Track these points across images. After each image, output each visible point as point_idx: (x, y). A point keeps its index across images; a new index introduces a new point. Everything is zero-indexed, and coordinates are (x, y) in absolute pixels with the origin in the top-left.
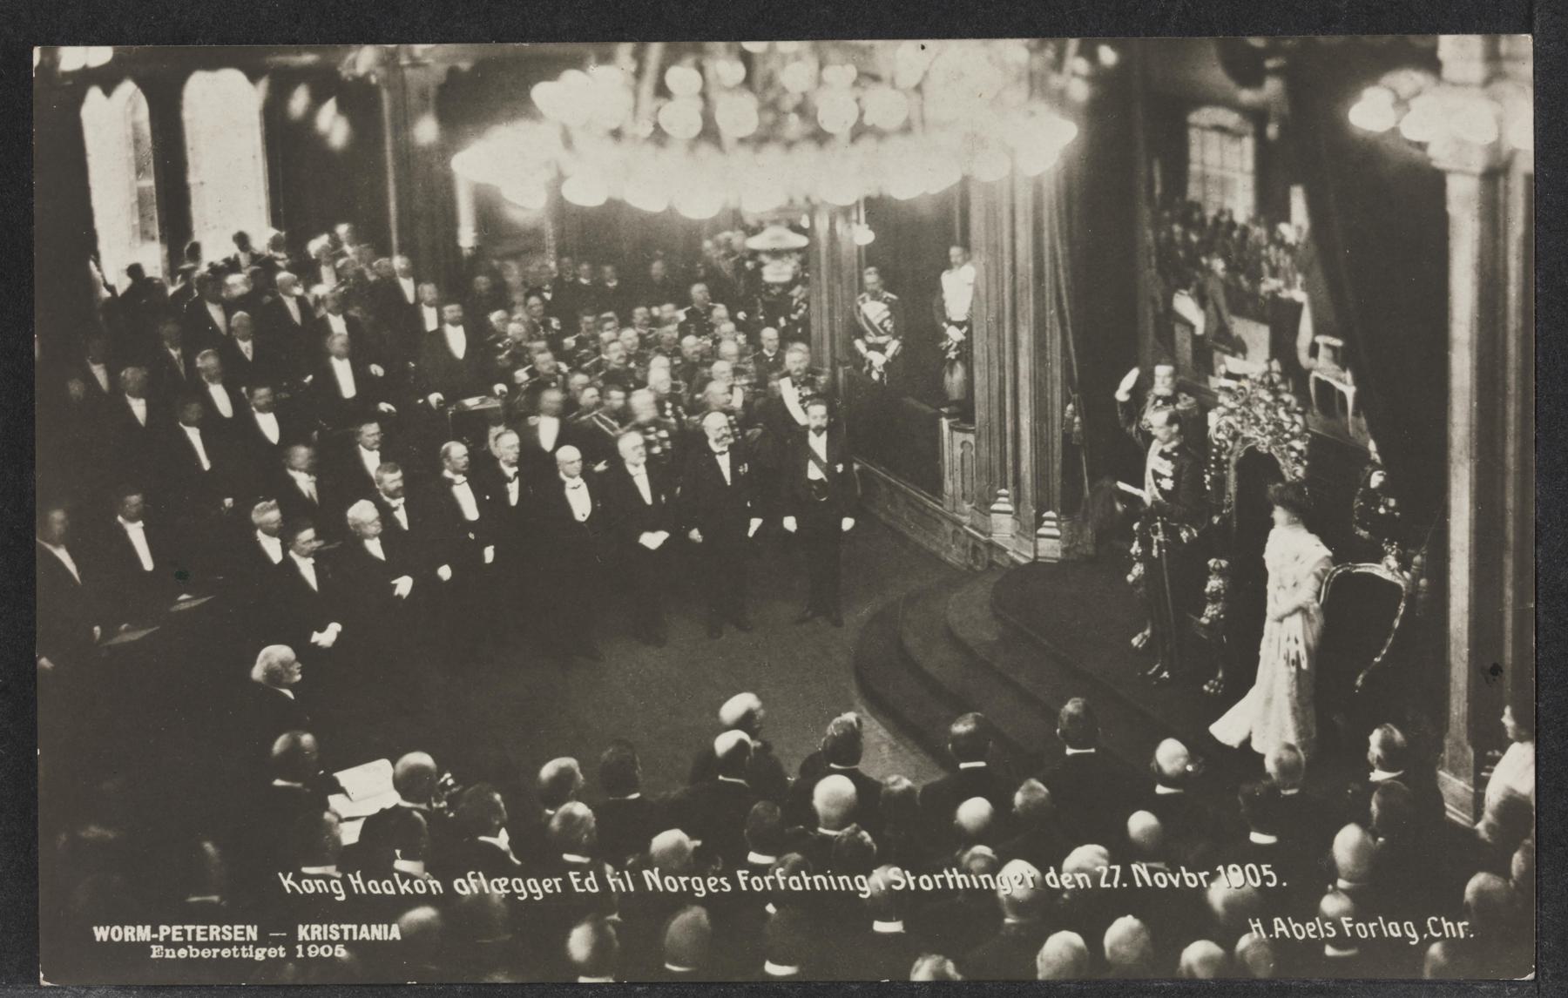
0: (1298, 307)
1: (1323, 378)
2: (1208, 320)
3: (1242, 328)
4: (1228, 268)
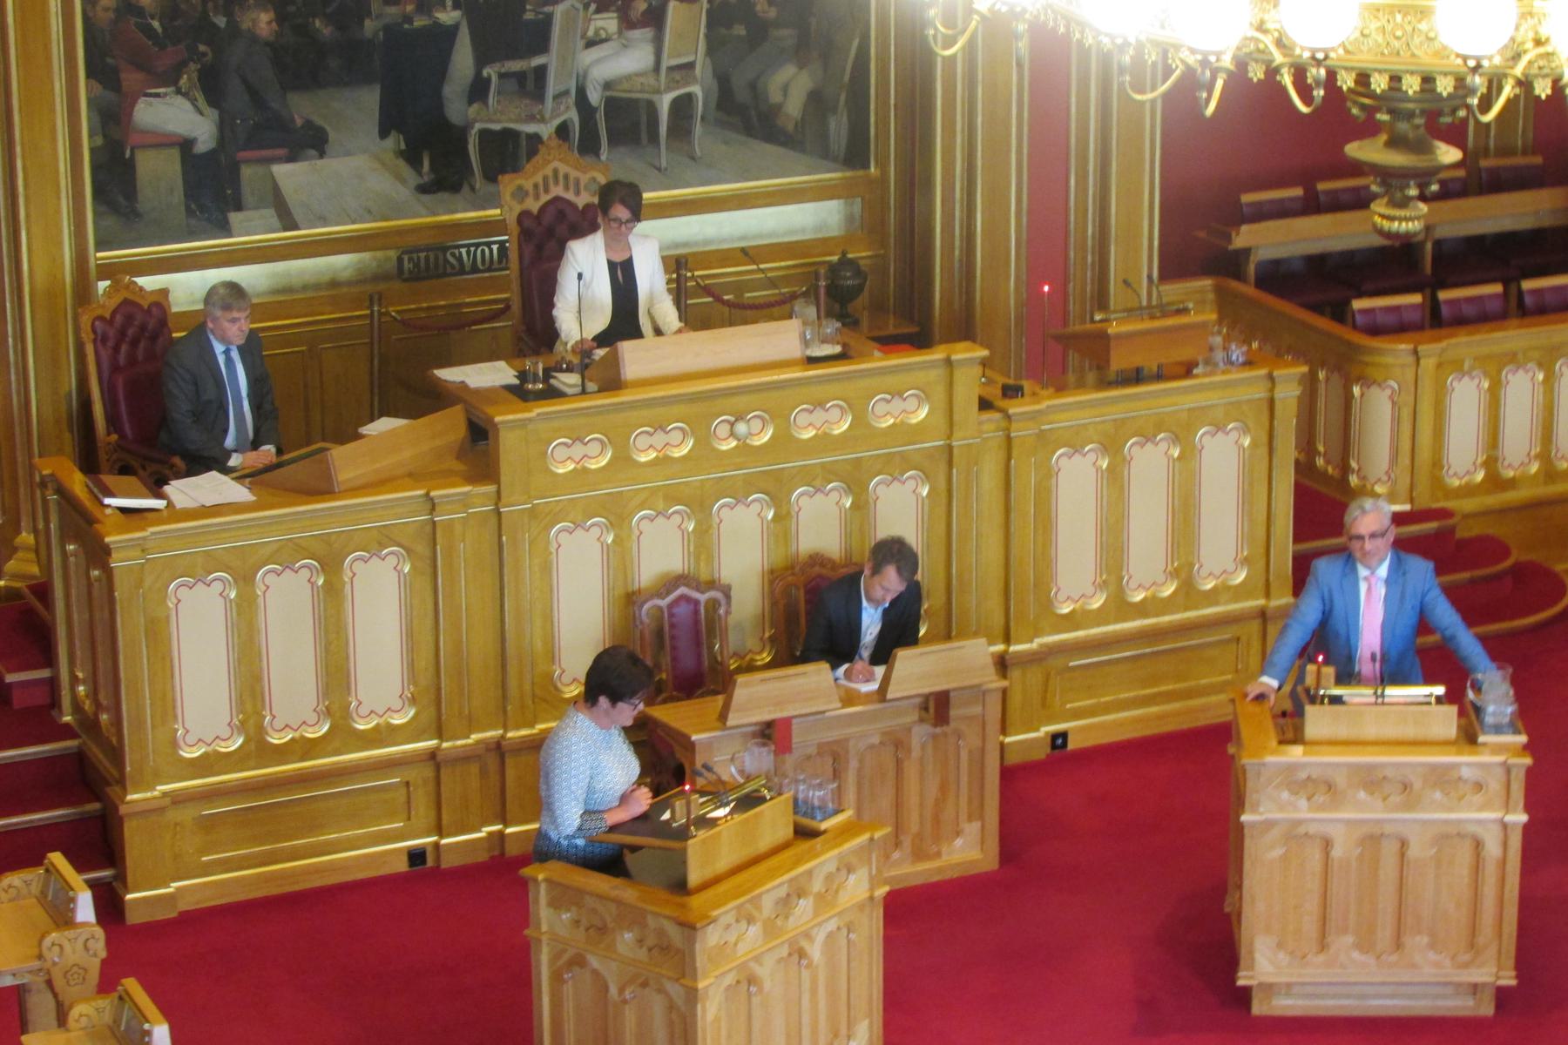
0: (452, 32)
1: (497, 127)
2: (222, 126)
3: (302, 107)
4: (281, 18)
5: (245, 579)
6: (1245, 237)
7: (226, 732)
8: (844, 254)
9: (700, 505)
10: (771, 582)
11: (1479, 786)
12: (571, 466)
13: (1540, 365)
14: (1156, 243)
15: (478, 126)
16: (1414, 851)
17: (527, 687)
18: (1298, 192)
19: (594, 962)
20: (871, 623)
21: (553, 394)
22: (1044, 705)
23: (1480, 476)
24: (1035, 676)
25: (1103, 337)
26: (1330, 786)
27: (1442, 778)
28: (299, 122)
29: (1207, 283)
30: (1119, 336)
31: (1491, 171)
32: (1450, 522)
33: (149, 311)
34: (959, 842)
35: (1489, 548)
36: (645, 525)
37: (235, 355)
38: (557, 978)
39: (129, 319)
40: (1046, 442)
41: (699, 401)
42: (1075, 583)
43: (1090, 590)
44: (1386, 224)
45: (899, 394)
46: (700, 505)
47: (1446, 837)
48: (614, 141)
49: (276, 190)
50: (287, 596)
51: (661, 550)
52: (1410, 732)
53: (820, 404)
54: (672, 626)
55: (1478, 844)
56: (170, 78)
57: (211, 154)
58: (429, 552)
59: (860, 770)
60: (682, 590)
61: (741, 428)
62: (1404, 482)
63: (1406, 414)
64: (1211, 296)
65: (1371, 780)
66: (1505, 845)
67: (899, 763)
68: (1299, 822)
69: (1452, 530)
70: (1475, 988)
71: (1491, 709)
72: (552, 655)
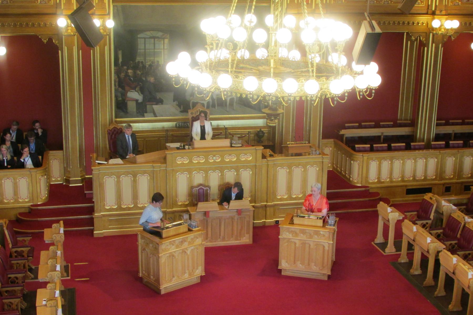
2: (144, 98)
5: (118, 177)
6: (343, 132)
7: (114, 204)
8: (261, 129)
9: (206, 171)
10: (219, 187)
11: (324, 235)
12: (181, 162)
13: (390, 160)
14: (321, 132)
15: (192, 101)
16: (312, 247)
17: (171, 202)
18: (357, 124)
19: (147, 250)
20: (233, 196)
21: (184, 149)
22: (274, 215)
23: (376, 181)
24: (272, 209)
25: (288, 147)
26: (296, 233)
27: (317, 233)
28: (158, 98)
29: (332, 140)
30: (290, 147)
31: (399, 123)
32: (368, 189)
33: (119, 129)
34: (244, 238)
35: (377, 194)
36: (195, 174)
37: (130, 137)
38: (142, 252)
39: (115, 130)
40: (275, 166)
41: (207, 152)
42: (282, 192)
43: (284, 194)
44: (270, 125)
45: (246, 154)
46: (206, 171)
47: (317, 244)
48: (218, 105)
49: (153, 109)
50: (126, 181)
51: (198, 179)
52: (314, 224)
53: (230, 155)
54: (199, 193)
55: (324, 247)
56: (134, 88)
57: (142, 103)
58: (153, 176)
59: (225, 223)
60: (201, 187)
61: (214, 158)
62: (360, 180)
63: (361, 167)
64: (333, 143)
65: (303, 232)
66: (329, 247)
67: (233, 222)
68: (290, 239)
69: (368, 190)
70: (324, 274)
71: (415, 228)
72: (176, 196)
